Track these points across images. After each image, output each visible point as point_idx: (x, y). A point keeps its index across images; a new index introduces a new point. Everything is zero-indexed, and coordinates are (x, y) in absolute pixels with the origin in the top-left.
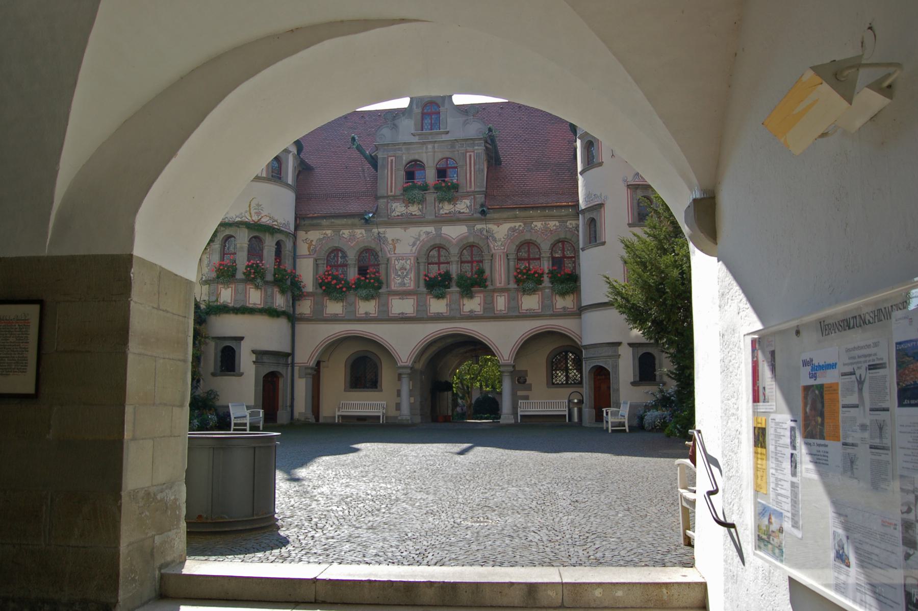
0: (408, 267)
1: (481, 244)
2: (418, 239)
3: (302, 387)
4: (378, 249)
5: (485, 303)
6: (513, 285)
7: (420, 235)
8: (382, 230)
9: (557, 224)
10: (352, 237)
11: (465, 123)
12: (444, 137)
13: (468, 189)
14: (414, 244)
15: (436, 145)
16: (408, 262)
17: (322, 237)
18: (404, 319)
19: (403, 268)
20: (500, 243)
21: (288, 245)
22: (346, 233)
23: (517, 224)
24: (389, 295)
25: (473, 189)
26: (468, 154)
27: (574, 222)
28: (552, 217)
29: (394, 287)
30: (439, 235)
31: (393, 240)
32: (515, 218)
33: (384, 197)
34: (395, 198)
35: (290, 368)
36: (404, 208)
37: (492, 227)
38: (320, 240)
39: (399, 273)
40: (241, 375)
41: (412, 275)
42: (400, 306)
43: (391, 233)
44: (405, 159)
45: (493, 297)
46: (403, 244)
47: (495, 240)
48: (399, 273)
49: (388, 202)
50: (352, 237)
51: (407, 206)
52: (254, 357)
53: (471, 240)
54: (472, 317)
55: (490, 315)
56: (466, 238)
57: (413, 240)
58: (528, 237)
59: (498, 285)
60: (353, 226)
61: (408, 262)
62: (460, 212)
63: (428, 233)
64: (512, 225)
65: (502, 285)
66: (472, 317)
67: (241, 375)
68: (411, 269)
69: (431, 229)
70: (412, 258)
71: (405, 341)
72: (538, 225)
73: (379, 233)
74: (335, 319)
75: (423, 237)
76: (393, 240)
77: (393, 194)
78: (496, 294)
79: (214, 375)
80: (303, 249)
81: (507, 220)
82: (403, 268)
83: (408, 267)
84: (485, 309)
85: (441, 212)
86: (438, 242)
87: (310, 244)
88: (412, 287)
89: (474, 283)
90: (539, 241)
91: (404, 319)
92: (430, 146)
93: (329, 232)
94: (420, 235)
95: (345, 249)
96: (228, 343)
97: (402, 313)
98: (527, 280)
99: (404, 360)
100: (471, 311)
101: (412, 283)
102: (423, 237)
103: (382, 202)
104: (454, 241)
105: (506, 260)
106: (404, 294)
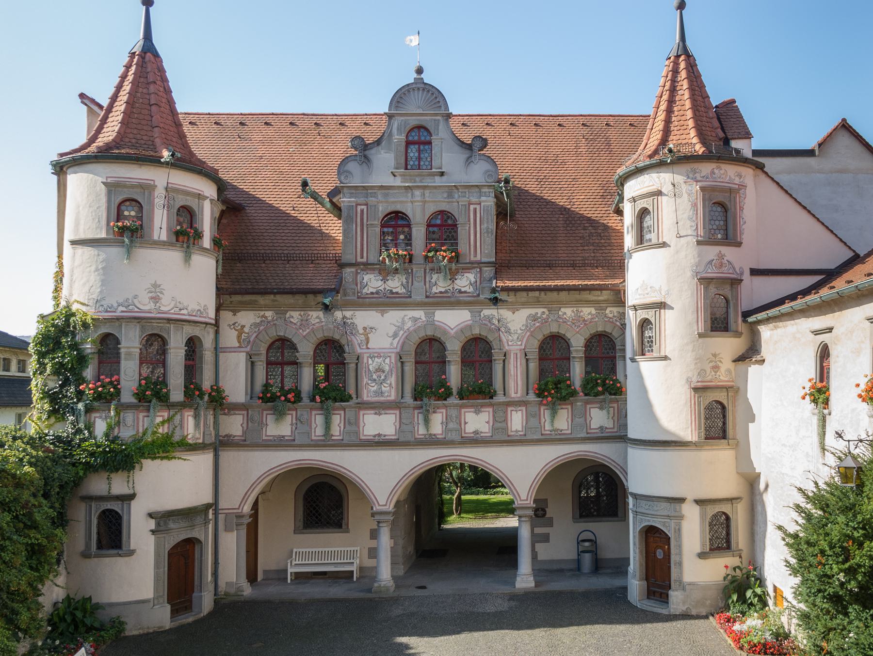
0: (387, 368)
1: (490, 338)
2: (400, 328)
3: (232, 545)
4: (343, 342)
5: (495, 420)
6: (532, 397)
7: (403, 323)
8: (348, 314)
9: (593, 311)
10: (304, 323)
11: (469, 161)
12: (438, 181)
13: (473, 258)
14: (395, 335)
15: (427, 192)
16: (387, 361)
17: (258, 320)
18: (380, 443)
19: (380, 370)
20: (515, 337)
21: (208, 341)
22: (295, 316)
23: (540, 311)
24: (360, 409)
25: (478, 258)
26: (472, 207)
27: (615, 310)
28: (588, 303)
29: (366, 397)
30: (431, 323)
31: (365, 329)
32: (537, 303)
33: (351, 265)
34: (367, 266)
35: (211, 527)
36: (380, 283)
37: (505, 313)
38: (256, 325)
39: (375, 377)
40: (131, 553)
41: (393, 380)
42: (376, 424)
43: (362, 318)
44: (383, 209)
45: (506, 412)
46: (380, 335)
47: (508, 331)
48: (375, 377)
49: (357, 273)
50: (304, 323)
51: (385, 280)
52: (152, 524)
53: (476, 331)
54: (476, 441)
55: (501, 438)
56: (470, 327)
57: (394, 329)
58: (554, 329)
59: (513, 395)
60: (305, 307)
61: (387, 361)
62: (460, 292)
63: (415, 320)
64: (533, 311)
65: (519, 395)
66: (476, 441)
67: (131, 553)
68: (391, 370)
69: (420, 314)
70: (393, 355)
71: (382, 476)
72: (568, 312)
73: (344, 317)
74: (280, 444)
75: (409, 324)
76: (365, 329)
77: (364, 260)
78: (509, 409)
79: (86, 555)
80: (229, 338)
81: (525, 305)
82: (380, 370)
83: (387, 368)
84: (494, 429)
85: (434, 290)
86: (430, 333)
87: (241, 332)
88: (393, 398)
89: (480, 390)
90: (568, 335)
91: (380, 443)
92: (417, 193)
93: (269, 314)
94: (403, 323)
95: (295, 340)
96: (109, 505)
97: (379, 435)
98: (551, 387)
99: (382, 501)
100: (476, 432)
101: (393, 391)
102: (409, 324)
103: (348, 272)
104: (452, 332)
105: (524, 361)
106: (380, 407)
